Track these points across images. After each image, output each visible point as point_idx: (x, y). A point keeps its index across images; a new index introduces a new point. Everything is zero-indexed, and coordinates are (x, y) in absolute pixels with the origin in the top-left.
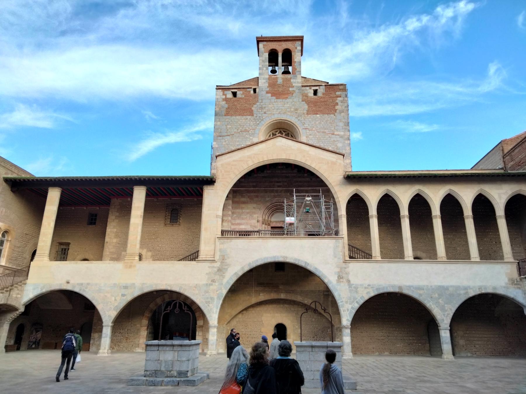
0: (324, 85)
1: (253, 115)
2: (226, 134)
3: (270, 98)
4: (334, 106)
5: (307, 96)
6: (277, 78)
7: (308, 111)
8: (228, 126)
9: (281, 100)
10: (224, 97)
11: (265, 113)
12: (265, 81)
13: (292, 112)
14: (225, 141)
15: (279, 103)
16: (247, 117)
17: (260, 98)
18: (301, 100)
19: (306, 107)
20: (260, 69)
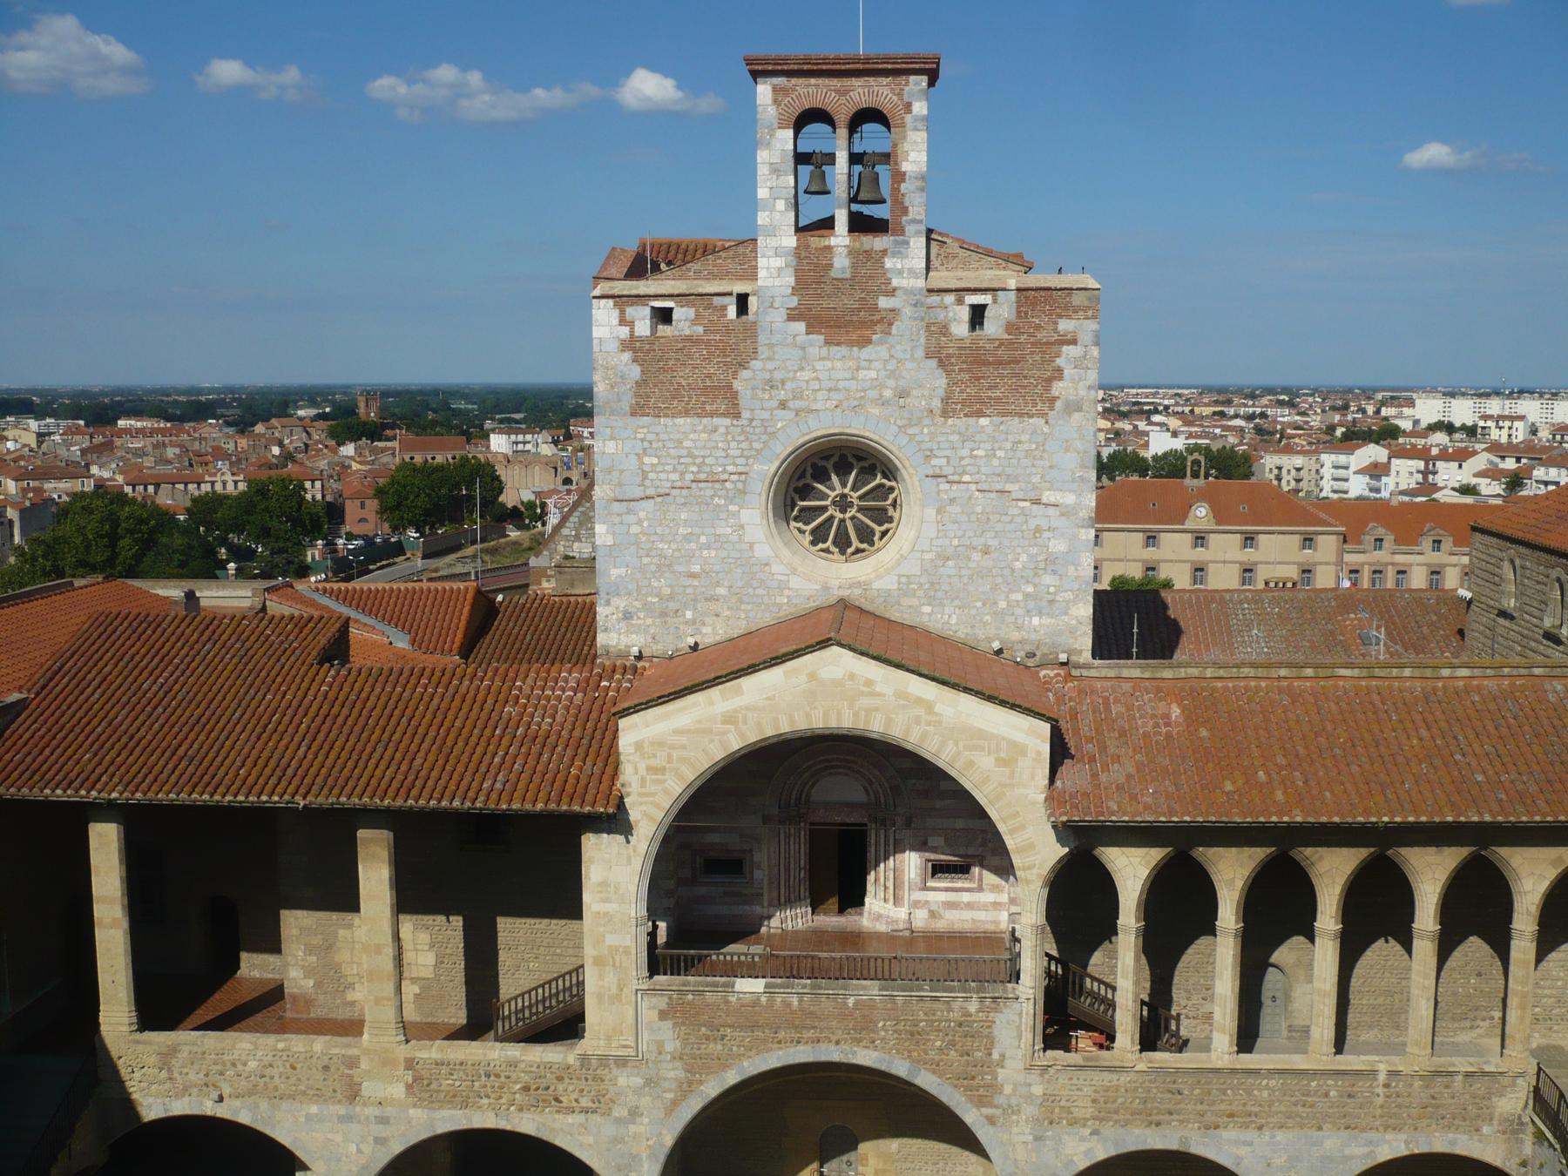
0: (1012, 284)
2: (639, 493)
3: (803, 338)
4: (1049, 380)
5: (944, 329)
6: (829, 248)
7: (946, 400)
8: (647, 460)
9: (843, 350)
10: (624, 332)
11: (783, 405)
12: (779, 262)
13: (885, 403)
14: (639, 522)
15: (839, 364)
16: (716, 421)
17: (762, 339)
18: (920, 353)
19: (941, 382)
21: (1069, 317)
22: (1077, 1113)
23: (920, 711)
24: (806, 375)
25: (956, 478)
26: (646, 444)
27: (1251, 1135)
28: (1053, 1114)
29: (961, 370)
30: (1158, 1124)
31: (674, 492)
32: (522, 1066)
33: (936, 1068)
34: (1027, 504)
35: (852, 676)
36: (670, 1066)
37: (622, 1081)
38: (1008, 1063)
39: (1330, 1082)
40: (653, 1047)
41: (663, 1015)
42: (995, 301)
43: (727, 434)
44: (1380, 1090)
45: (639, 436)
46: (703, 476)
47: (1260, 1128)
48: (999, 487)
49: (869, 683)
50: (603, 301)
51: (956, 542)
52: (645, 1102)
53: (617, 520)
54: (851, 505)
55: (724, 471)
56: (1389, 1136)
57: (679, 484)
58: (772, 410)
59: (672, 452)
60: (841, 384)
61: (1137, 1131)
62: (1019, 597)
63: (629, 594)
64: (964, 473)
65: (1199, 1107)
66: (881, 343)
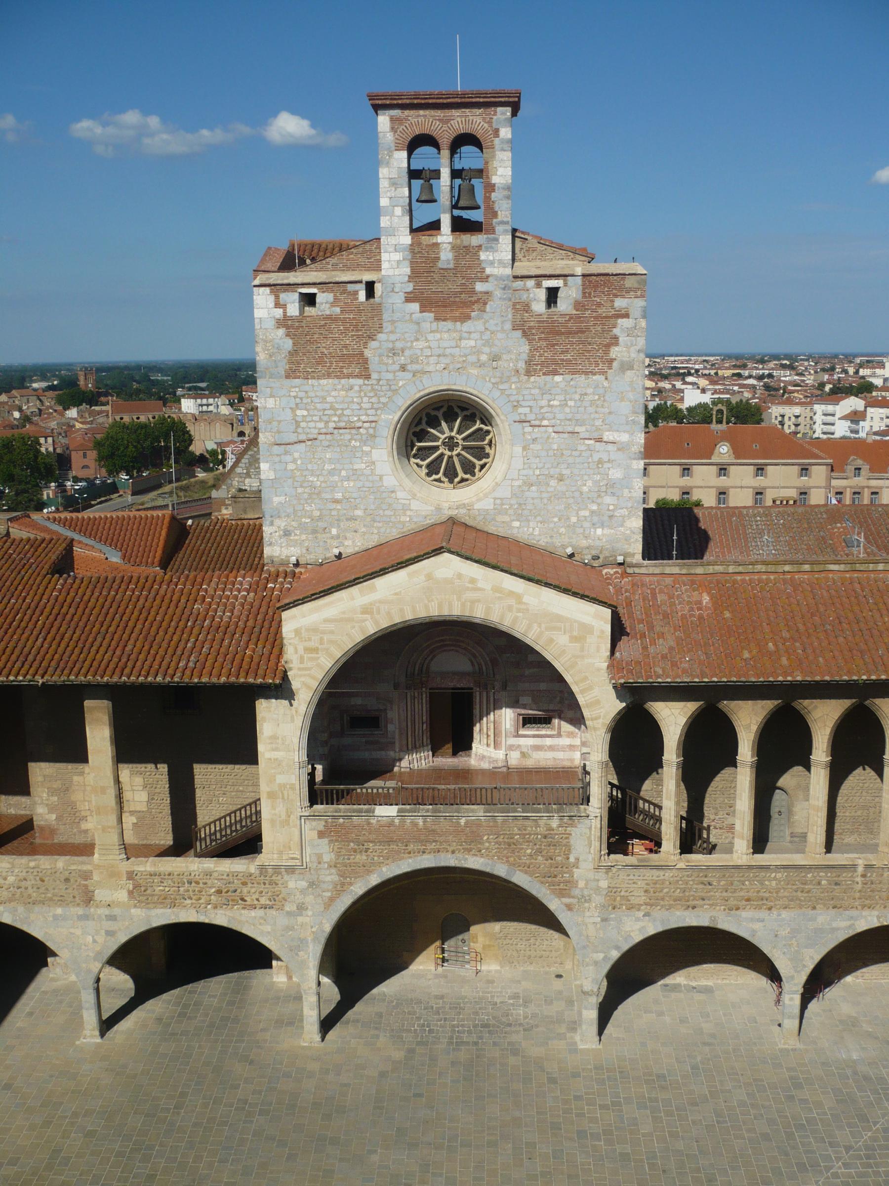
0: (579, 271)
1: (368, 377)
2: (293, 438)
3: (417, 316)
4: (608, 346)
6: (437, 245)
7: (528, 363)
8: (299, 413)
9: (449, 324)
10: (279, 313)
11: (403, 368)
12: (398, 256)
14: (294, 461)
15: (446, 336)
16: (352, 381)
17: (386, 316)
18: (508, 326)
21: (623, 297)
22: (634, 900)
23: (512, 602)
24: (421, 344)
25: (537, 423)
26: (298, 400)
27: (763, 914)
28: (616, 902)
29: (540, 339)
30: (694, 907)
31: (321, 437)
32: (215, 875)
33: (527, 869)
34: (592, 442)
35: (460, 576)
37: (291, 885)
38: (582, 864)
39: (821, 874)
40: (314, 859)
41: (321, 835)
42: (566, 284)
43: (360, 391)
44: (859, 879)
45: (293, 394)
46: (342, 424)
47: (770, 909)
48: (570, 429)
49: (473, 581)
50: (262, 289)
51: (537, 472)
52: (309, 899)
53: (277, 459)
54: (457, 444)
55: (359, 420)
56: (866, 913)
57: (324, 431)
58: (394, 372)
59: (318, 406)
60: (448, 351)
61: (678, 913)
62: (587, 513)
63: (288, 516)
64: (544, 418)
65: (725, 894)
66: (478, 318)
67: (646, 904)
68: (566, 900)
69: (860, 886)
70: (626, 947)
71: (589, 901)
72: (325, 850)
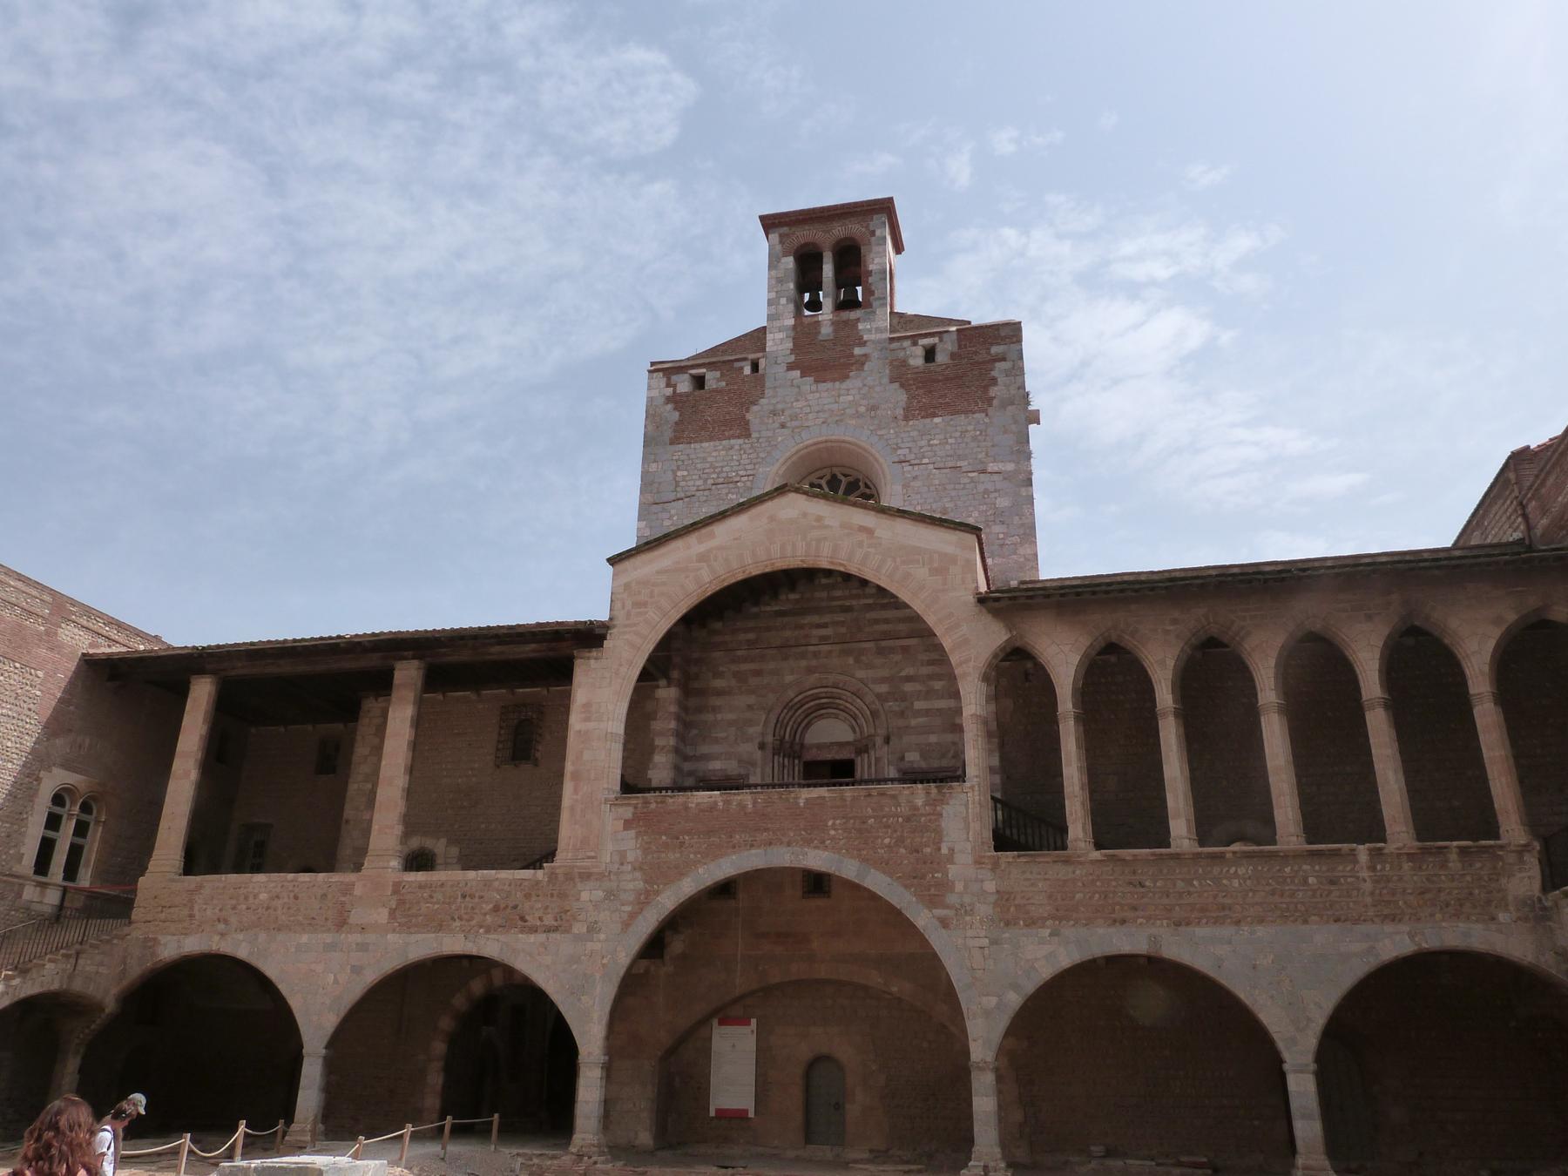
2: (672, 496)
3: (798, 381)
4: (986, 388)
5: (904, 363)
7: (907, 409)
9: (829, 385)
11: (783, 426)
18: (886, 380)
19: (902, 397)
20: (770, 303)
23: (863, 537)
24: (799, 404)
27: (1227, 931)
28: (1011, 913)
30: (1123, 922)
32: (496, 884)
33: (885, 865)
35: (805, 515)
36: (629, 877)
37: (585, 896)
38: (959, 858)
39: (1305, 867)
40: (616, 858)
41: (628, 825)
42: (941, 340)
44: (1365, 874)
47: (1238, 923)
49: (819, 519)
56: (1389, 928)
61: (1101, 931)
65: (1166, 901)
67: (1054, 918)
68: (939, 912)
69: (1368, 886)
70: (1030, 987)
71: (971, 912)
72: (630, 844)
